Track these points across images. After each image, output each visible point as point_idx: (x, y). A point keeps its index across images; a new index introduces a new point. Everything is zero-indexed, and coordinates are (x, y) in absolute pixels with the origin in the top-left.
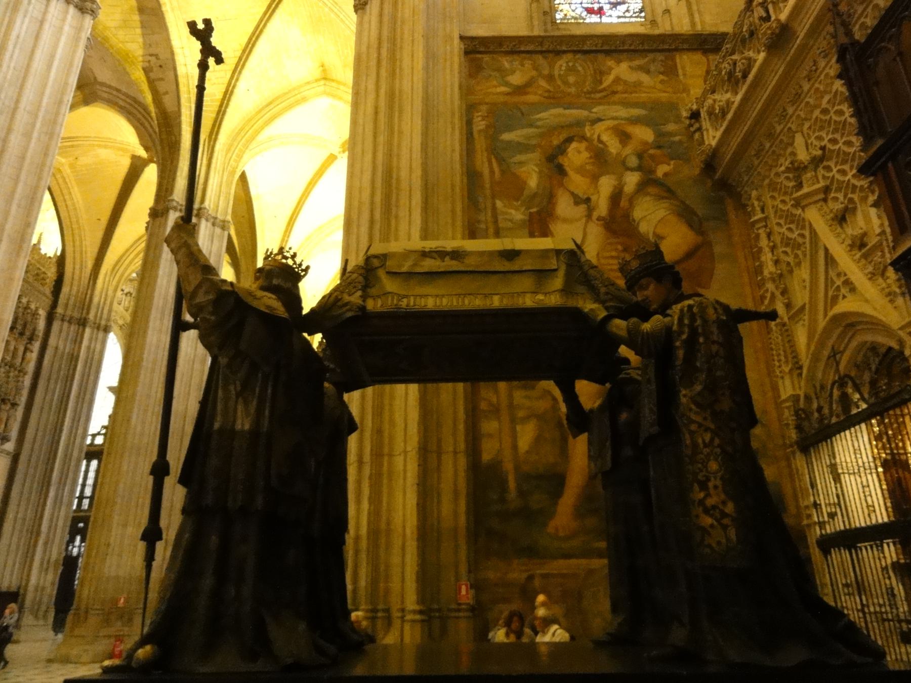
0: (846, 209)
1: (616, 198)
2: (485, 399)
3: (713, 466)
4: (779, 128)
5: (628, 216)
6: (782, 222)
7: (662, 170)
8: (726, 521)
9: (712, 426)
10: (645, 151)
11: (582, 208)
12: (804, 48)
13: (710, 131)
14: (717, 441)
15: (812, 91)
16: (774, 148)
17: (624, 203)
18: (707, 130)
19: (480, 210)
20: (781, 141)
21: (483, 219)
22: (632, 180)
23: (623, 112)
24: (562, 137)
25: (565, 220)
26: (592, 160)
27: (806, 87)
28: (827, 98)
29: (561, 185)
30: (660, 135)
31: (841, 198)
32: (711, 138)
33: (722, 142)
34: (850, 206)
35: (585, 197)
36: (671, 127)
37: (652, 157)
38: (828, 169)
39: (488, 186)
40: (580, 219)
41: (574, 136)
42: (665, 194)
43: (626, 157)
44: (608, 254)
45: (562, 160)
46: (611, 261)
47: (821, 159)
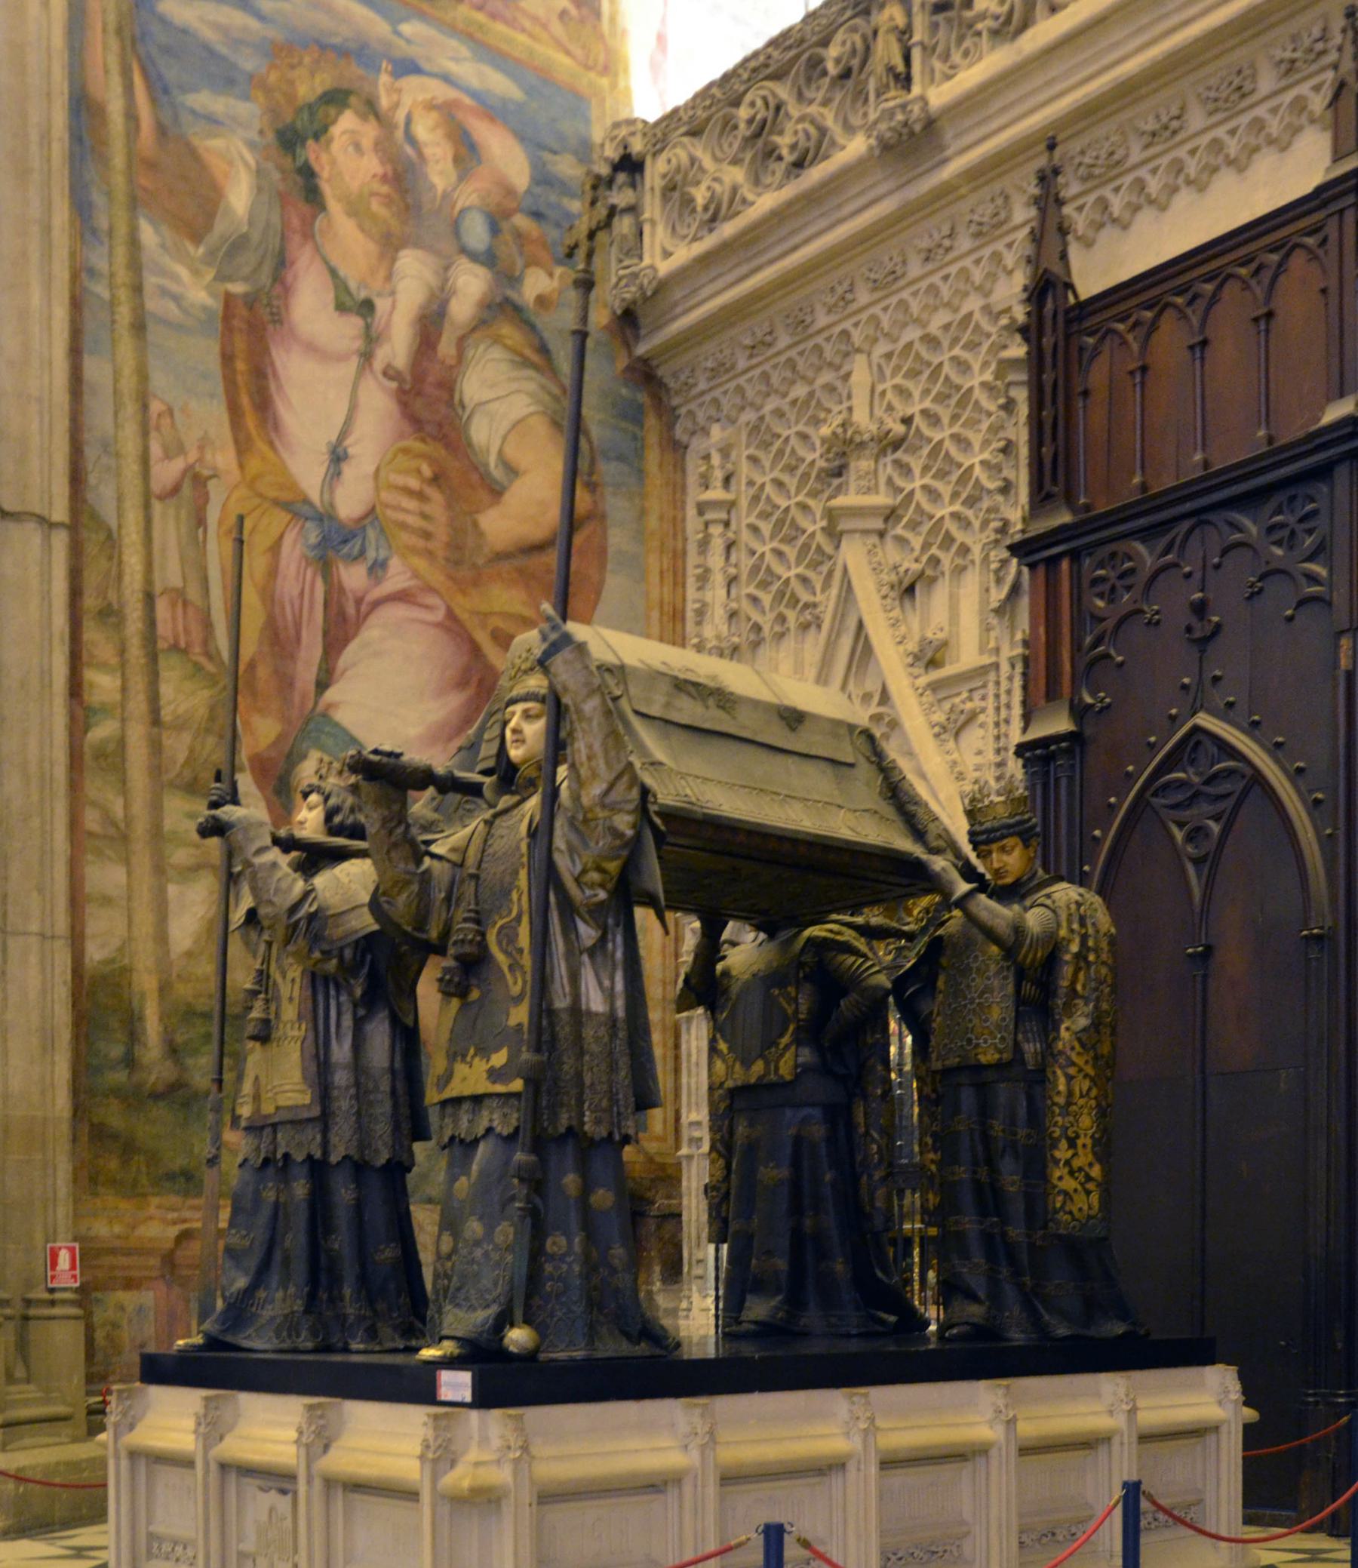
0: (922, 573)
1: (430, 324)
2: (94, 804)
3: (1086, 1121)
4: (822, 320)
5: (451, 391)
6: (766, 528)
7: (536, 284)
8: (1090, 1186)
9: (1092, 1073)
10: (507, 215)
11: (353, 324)
12: (945, 193)
13: (660, 229)
14: (1094, 1092)
15: (924, 285)
16: (793, 353)
17: (446, 347)
18: (653, 223)
19: (94, 232)
20: (818, 349)
21: (102, 265)
22: (471, 285)
23: (471, 71)
24: (323, 82)
25: (312, 349)
26: (385, 189)
27: (915, 269)
28: (942, 318)
29: (308, 235)
30: (543, 178)
31: (917, 542)
32: (658, 251)
33: (682, 274)
34: (929, 572)
35: (363, 295)
36: (567, 168)
37: (519, 235)
38: (905, 470)
39: (119, 161)
40: (342, 358)
41: (347, 93)
42: (535, 358)
43: (462, 211)
44: (400, 480)
45: (311, 151)
46: (411, 504)
47: (897, 444)
